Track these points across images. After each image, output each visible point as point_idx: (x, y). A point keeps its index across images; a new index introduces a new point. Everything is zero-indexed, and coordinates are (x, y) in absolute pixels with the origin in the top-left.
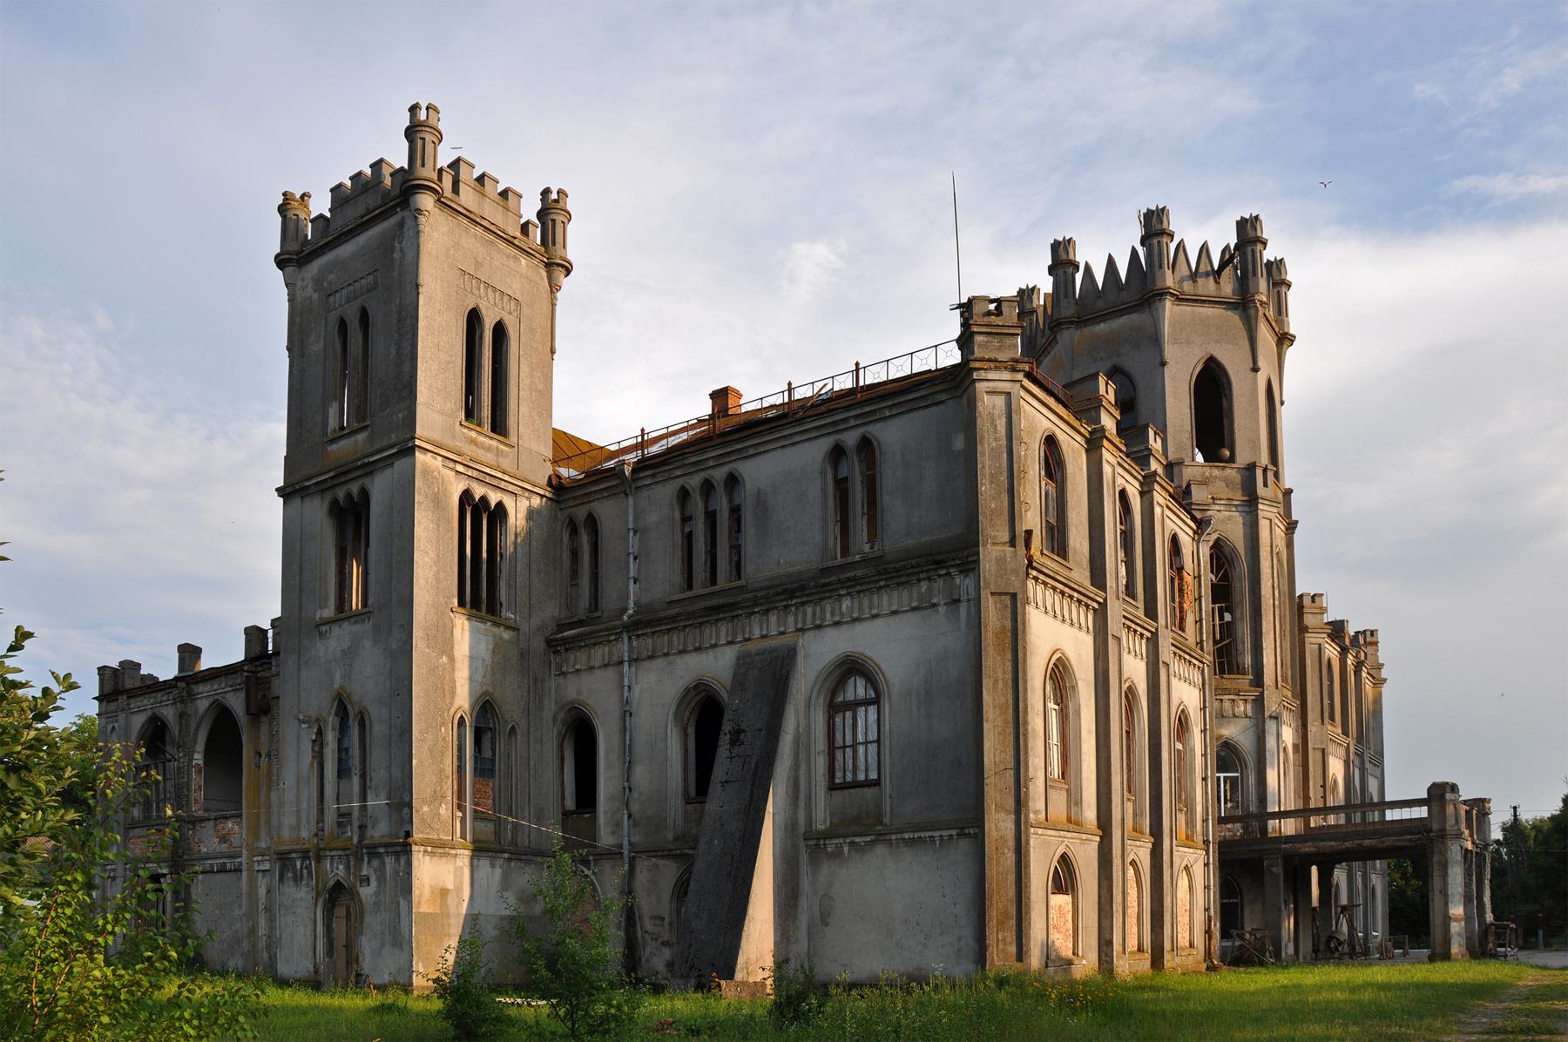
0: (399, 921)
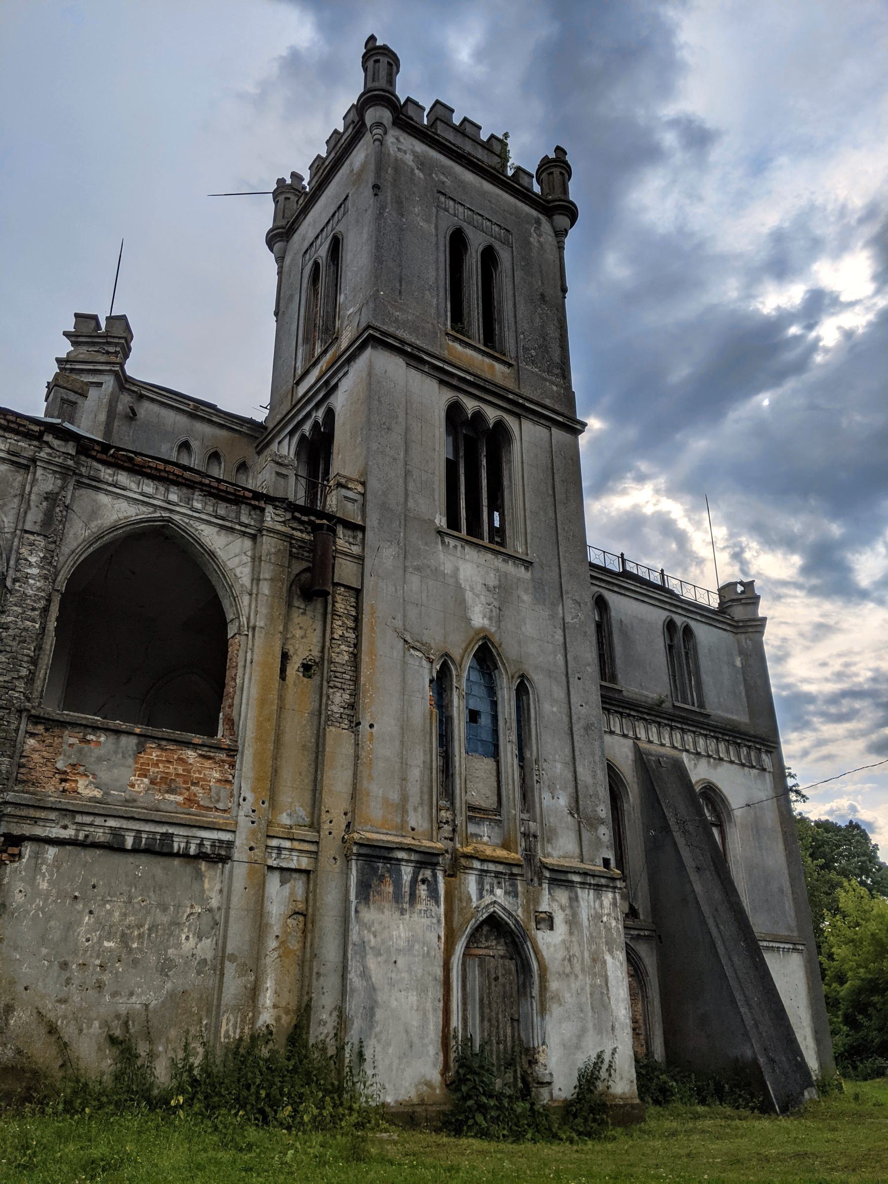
0: (608, 990)
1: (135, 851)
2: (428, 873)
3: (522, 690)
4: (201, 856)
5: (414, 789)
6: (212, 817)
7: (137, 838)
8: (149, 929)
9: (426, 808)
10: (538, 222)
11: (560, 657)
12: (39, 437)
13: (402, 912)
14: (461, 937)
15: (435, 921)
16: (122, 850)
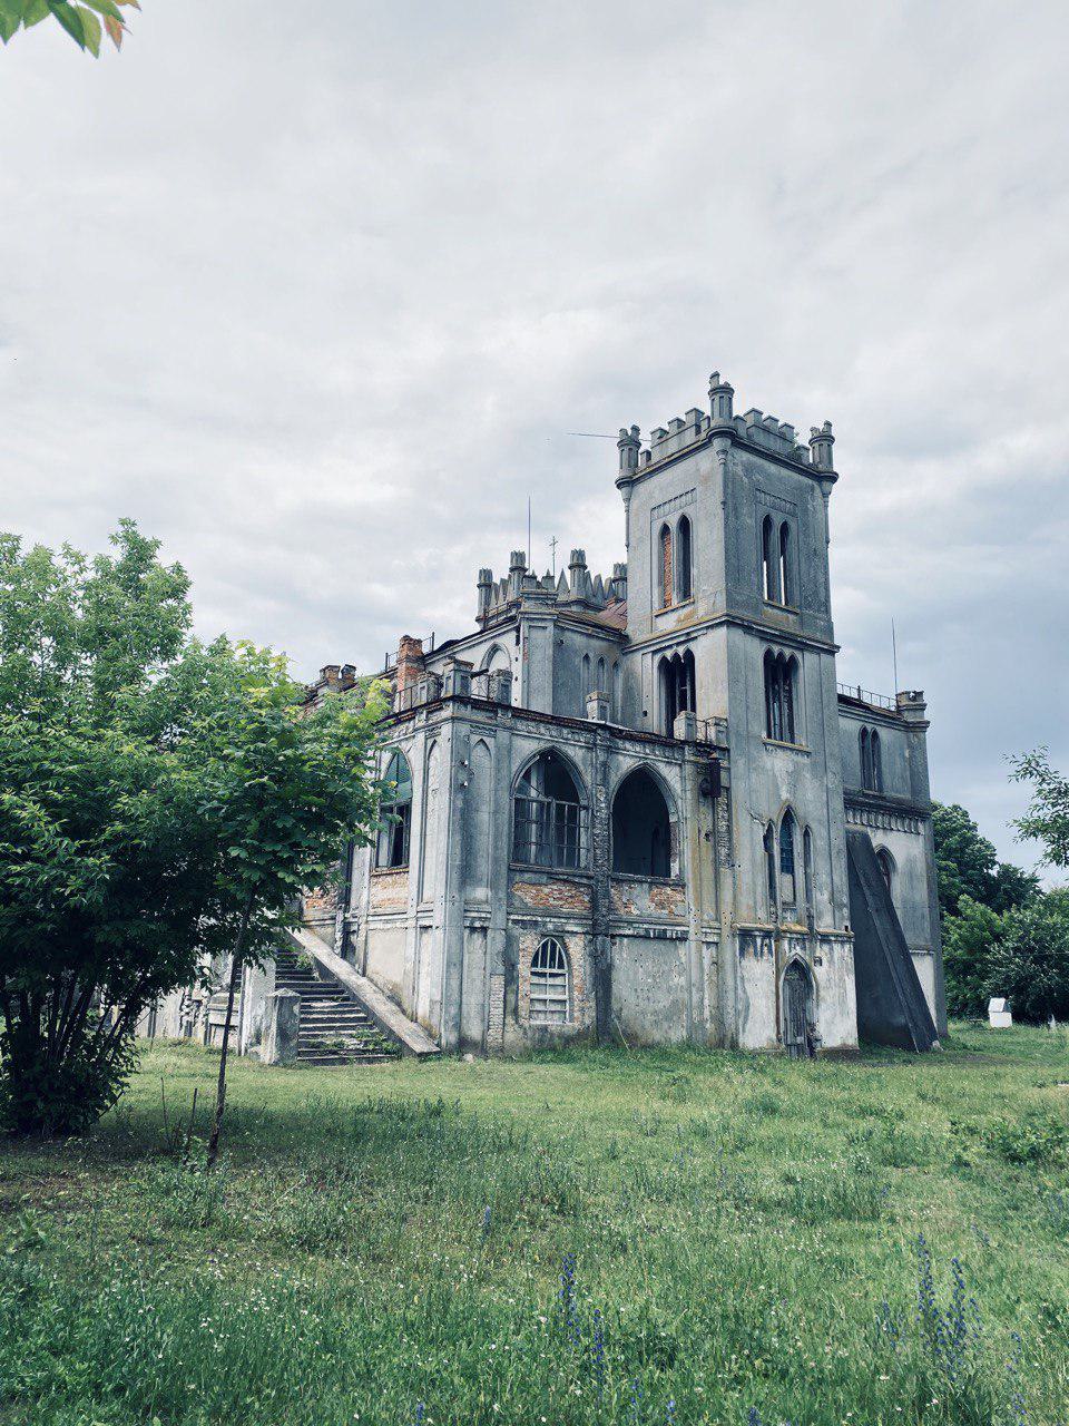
3: (806, 834)
4: (677, 938)
5: (759, 899)
6: (680, 920)
10: (813, 489)
11: (825, 811)
12: (595, 731)
16: (649, 938)
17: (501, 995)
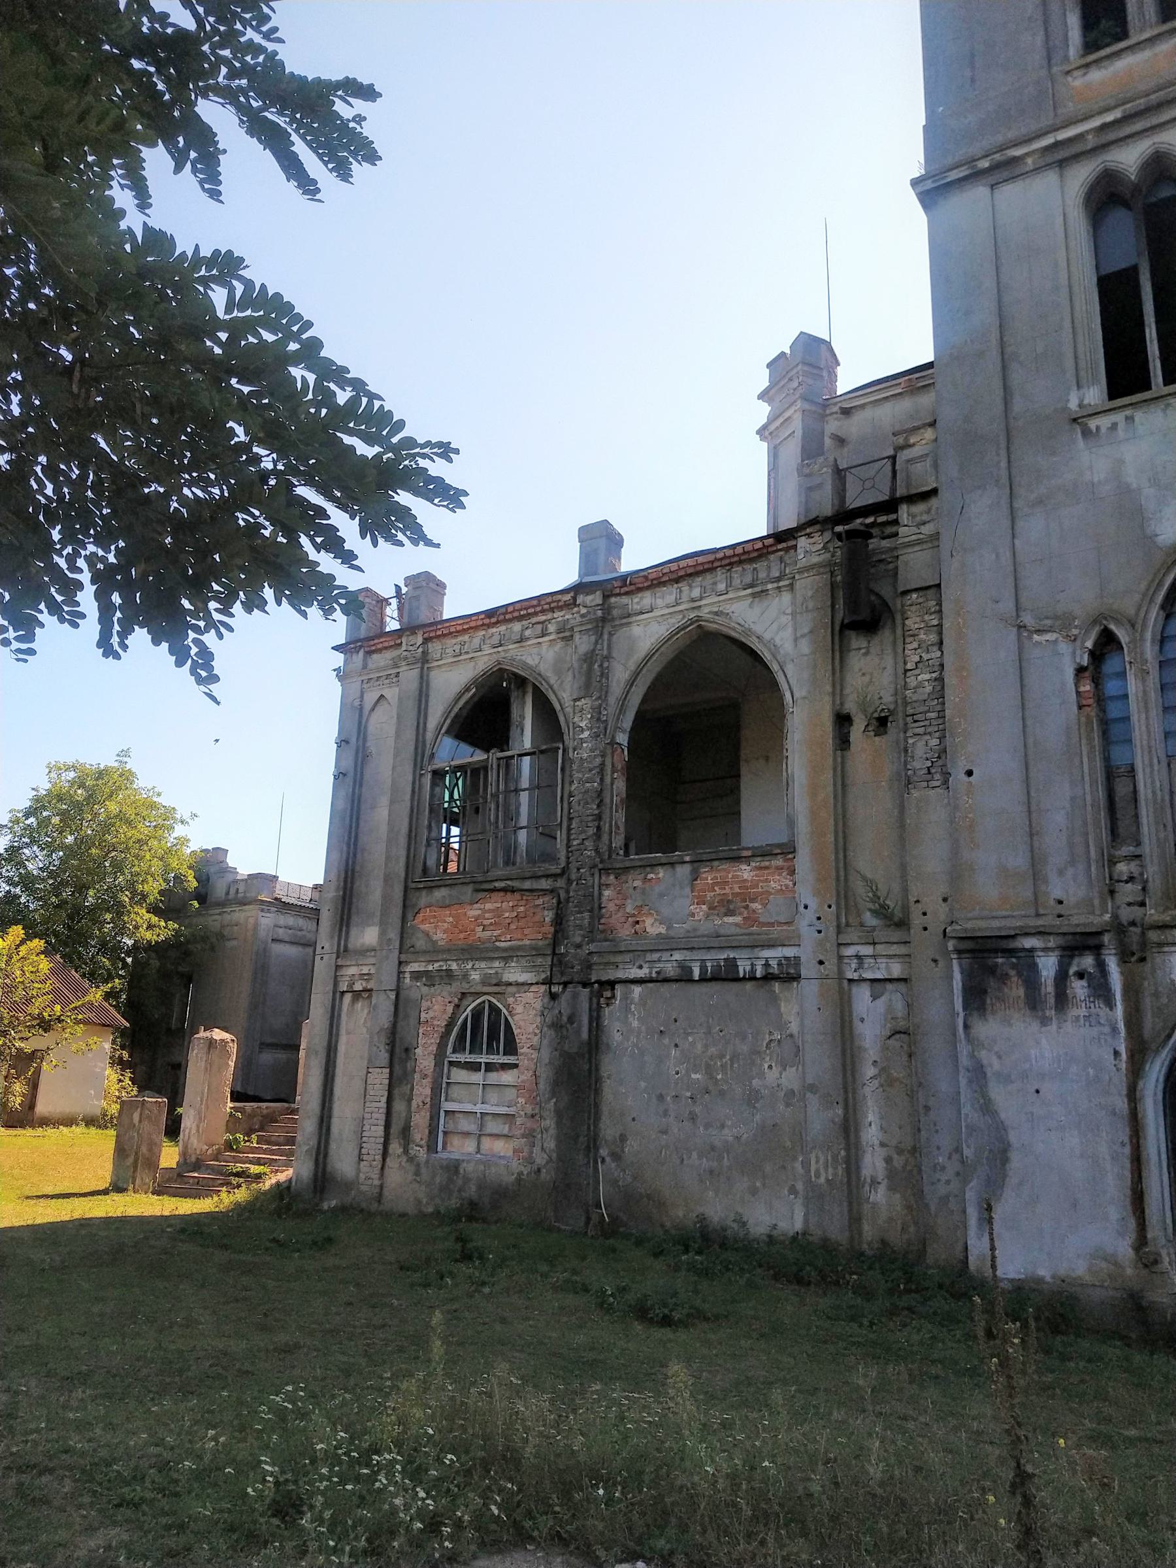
1: (703, 979)
2: (1087, 962)
4: (768, 978)
6: (776, 932)
7: (703, 969)
8: (731, 1060)
9: (1081, 867)
12: (574, 603)
13: (1045, 1022)
14: (1157, 1052)
15: (1107, 1030)
16: (691, 980)
17: (383, 1104)
